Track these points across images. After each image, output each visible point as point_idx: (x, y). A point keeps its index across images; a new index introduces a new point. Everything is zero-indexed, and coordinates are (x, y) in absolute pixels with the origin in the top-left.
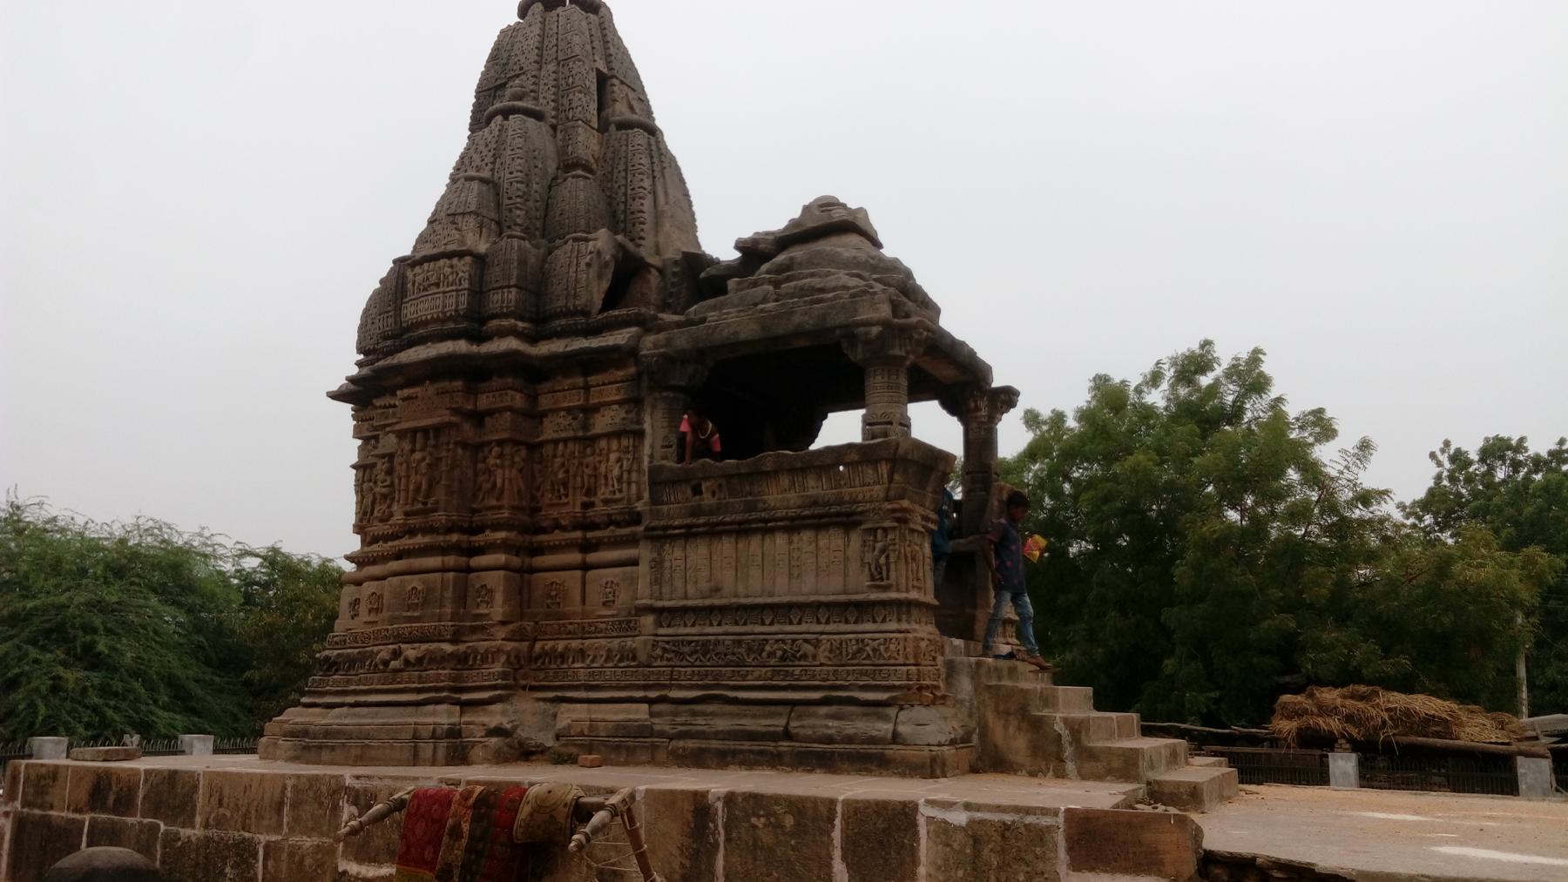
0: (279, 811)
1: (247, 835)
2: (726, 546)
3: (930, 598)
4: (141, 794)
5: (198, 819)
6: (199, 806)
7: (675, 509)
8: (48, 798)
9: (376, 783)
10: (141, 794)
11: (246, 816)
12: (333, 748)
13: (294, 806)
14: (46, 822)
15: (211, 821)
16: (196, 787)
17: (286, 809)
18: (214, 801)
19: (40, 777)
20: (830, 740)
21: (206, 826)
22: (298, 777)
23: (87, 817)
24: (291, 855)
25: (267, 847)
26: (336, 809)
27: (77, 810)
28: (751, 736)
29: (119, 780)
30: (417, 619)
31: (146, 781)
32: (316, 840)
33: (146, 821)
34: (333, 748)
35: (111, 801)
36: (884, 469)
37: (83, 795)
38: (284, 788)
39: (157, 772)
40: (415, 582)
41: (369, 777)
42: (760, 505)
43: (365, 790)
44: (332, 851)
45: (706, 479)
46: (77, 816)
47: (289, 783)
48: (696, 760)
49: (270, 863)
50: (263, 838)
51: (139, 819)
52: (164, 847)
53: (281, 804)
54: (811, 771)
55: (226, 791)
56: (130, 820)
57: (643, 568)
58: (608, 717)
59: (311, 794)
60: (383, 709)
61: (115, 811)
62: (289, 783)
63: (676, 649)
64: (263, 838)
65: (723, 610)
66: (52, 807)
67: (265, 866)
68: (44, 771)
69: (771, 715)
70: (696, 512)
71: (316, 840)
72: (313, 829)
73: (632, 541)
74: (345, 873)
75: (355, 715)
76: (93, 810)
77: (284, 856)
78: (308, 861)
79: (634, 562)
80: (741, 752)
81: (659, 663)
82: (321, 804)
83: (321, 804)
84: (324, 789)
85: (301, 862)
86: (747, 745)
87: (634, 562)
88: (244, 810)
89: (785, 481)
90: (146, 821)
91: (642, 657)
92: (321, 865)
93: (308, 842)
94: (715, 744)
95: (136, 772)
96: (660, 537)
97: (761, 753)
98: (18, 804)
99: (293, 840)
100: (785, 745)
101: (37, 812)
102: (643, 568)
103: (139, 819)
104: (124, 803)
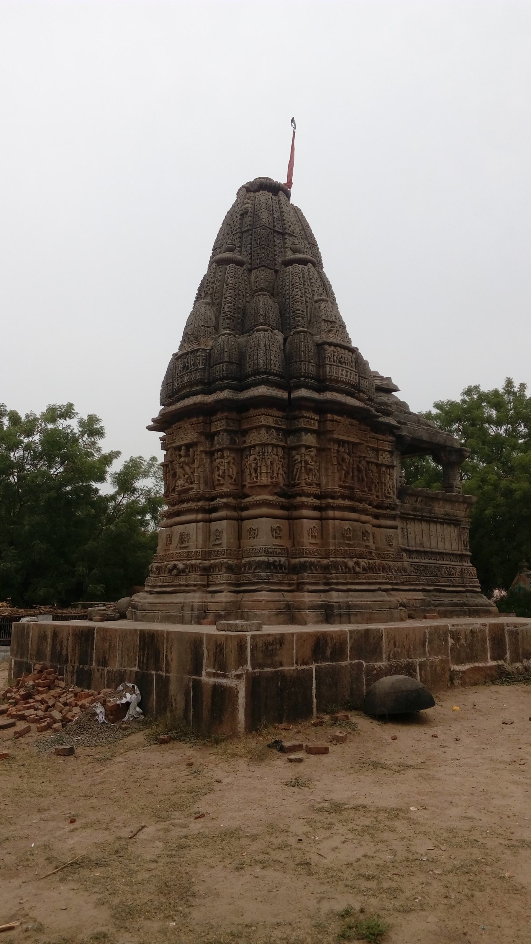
0: (424, 645)
1: (410, 660)
2: (424, 526)
3: (468, 553)
4: (348, 646)
5: (384, 656)
6: (384, 648)
7: (409, 505)
8: (277, 659)
9: (460, 627)
10: (348, 646)
11: (409, 650)
12: (356, 615)
13: (429, 643)
14: (281, 676)
15: (391, 656)
16: (381, 638)
17: (427, 644)
18: (392, 644)
19: (267, 644)
20: (477, 606)
21: (389, 659)
22: (430, 627)
23: (313, 667)
24: (431, 666)
25: (420, 665)
26: (446, 641)
27: (304, 663)
28: (457, 605)
29: (332, 638)
30: (349, 545)
31: (351, 637)
32: (440, 657)
33: (354, 662)
34: (356, 615)
35: (329, 652)
36: (466, 506)
37: (307, 651)
38: (425, 633)
39: (358, 631)
40: (347, 525)
41: (457, 625)
42: (433, 511)
43: (456, 631)
44: (446, 662)
45: (421, 496)
46: (305, 667)
47: (427, 631)
48: (444, 615)
49: (423, 672)
50: (418, 660)
51: (349, 661)
52: (367, 676)
53: (424, 642)
54: (475, 617)
55: (397, 639)
56: (344, 663)
57: (399, 530)
58: (417, 598)
59: (436, 636)
60: (364, 593)
61: (332, 659)
62: (427, 631)
63: (417, 568)
64: (418, 660)
65: (425, 552)
66: (281, 664)
67: (421, 675)
68: (271, 639)
69: (455, 597)
70: (415, 509)
71: (440, 657)
72: (439, 652)
73: (394, 518)
74: (454, 670)
75: (352, 596)
76: (316, 661)
77: (428, 668)
78: (438, 668)
79: (395, 528)
80: (456, 611)
81: (413, 574)
82: (440, 639)
83: (440, 639)
84: (441, 632)
85: (436, 668)
86: (457, 609)
87: (395, 528)
88: (407, 647)
89: (441, 503)
90: (354, 662)
91: (409, 571)
92: (443, 669)
93: (437, 659)
94: (449, 608)
95: (343, 633)
96: (404, 517)
97: (461, 611)
98: (249, 667)
99: (431, 659)
100: (466, 608)
101: (268, 670)
102: (399, 530)
103: (349, 661)
104: (338, 653)
